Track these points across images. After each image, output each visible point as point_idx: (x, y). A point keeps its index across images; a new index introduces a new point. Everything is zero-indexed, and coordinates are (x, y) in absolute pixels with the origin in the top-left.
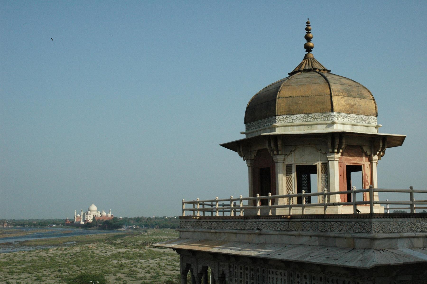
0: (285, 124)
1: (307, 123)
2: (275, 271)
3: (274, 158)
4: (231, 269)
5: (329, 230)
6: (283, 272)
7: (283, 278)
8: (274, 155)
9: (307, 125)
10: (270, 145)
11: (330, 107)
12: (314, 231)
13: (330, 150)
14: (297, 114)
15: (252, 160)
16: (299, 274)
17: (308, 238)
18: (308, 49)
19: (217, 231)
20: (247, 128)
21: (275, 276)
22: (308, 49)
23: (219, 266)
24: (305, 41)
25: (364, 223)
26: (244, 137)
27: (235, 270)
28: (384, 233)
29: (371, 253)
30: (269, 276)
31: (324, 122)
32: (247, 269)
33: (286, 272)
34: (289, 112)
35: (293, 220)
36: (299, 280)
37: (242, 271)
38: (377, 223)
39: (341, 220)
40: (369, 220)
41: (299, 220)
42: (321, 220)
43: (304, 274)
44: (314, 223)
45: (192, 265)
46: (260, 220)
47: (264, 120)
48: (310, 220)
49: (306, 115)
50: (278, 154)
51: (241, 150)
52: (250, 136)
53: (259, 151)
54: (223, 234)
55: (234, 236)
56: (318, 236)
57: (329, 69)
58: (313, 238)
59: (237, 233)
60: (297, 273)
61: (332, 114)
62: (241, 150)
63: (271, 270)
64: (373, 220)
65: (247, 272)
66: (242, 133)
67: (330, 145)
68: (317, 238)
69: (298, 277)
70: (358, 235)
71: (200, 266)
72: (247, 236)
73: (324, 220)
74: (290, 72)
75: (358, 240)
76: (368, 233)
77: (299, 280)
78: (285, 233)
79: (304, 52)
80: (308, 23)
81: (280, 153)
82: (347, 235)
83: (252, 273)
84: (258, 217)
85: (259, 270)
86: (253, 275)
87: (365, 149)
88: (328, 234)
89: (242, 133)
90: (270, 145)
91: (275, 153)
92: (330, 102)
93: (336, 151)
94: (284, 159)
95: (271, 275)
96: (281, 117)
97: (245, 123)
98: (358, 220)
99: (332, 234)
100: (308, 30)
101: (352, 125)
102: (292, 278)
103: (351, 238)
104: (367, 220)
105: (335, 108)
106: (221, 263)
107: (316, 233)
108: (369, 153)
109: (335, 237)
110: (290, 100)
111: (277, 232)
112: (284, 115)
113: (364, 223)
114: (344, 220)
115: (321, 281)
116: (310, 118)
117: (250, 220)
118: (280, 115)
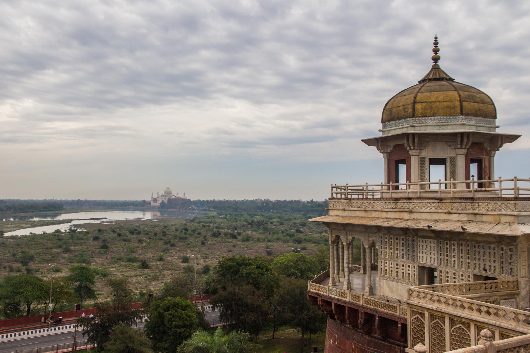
0: (421, 125)
1: (439, 124)
2: (424, 240)
3: (411, 152)
4: (382, 239)
5: (477, 209)
6: (432, 240)
7: (433, 245)
8: (411, 149)
9: (440, 125)
10: (408, 141)
11: (459, 111)
12: (463, 210)
13: (459, 146)
14: (430, 116)
15: (388, 153)
16: (448, 242)
17: (457, 215)
18: (436, 59)
19: (367, 209)
20: (384, 127)
21: (425, 244)
22: (436, 59)
23: (369, 237)
24: (433, 54)
25: (509, 203)
26: (380, 135)
27: (385, 240)
28: (525, 211)
29: (516, 226)
30: (419, 243)
31: (454, 123)
32: (397, 239)
33: (436, 241)
34: (424, 115)
35: (444, 201)
36: (448, 247)
37: (392, 241)
38: (520, 204)
39: (488, 201)
40: (514, 202)
41: (449, 201)
42: (470, 201)
43: (452, 242)
44: (463, 204)
45: (341, 236)
46: (411, 201)
47: (401, 121)
48: (459, 201)
49: (439, 117)
50: (414, 149)
51: (379, 145)
52: (386, 135)
53: (395, 146)
54: (373, 213)
55: (385, 213)
56: (467, 214)
57: (453, 78)
58: (461, 215)
59: (388, 211)
60: (446, 242)
61: (461, 117)
62: (379, 145)
63: (421, 240)
64: (517, 202)
65: (397, 241)
66: (380, 131)
67: (459, 143)
68: (466, 215)
69: (447, 244)
70: (504, 213)
71: (350, 238)
72: (398, 213)
73: (472, 201)
74: (420, 79)
75: (503, 217)
76: (513, 211)
77: (448, 247)
78: (435, 211)
79: (432, 63)
80: (436, 38)
81: (416, 148)
82: (493, 213)
83: (402, 242)
84: (410, 199)
85: (410, 240)
86: (403, 243)
87: (486, 145)
88: (476, 212)
89: (380, 131)
90: (408, 141)
91: (412, 148)
92: (459, 108)
93: (464, 147)
94: (419, 153)
95: (421, 244)
96: (417, 118)
97: (382, 122)
98: (504, 202)
99: (480, 212)
100: (436, 44)
101: (477, 126)
102: (441, 245)
103: (497, 215)
104: (512, 202)
105: (464, 113)
106: (371, 235)
107: (465, 211)
108: (488, 149)
109: (483, 214)
110: (424, 104)
111: (428, 211)
112: (420, 117)
113: (509, 203)
114: (491, 202)
115: (468, 246)
116: (442, 120)
117: (401, 201)
118: (417, 117)
